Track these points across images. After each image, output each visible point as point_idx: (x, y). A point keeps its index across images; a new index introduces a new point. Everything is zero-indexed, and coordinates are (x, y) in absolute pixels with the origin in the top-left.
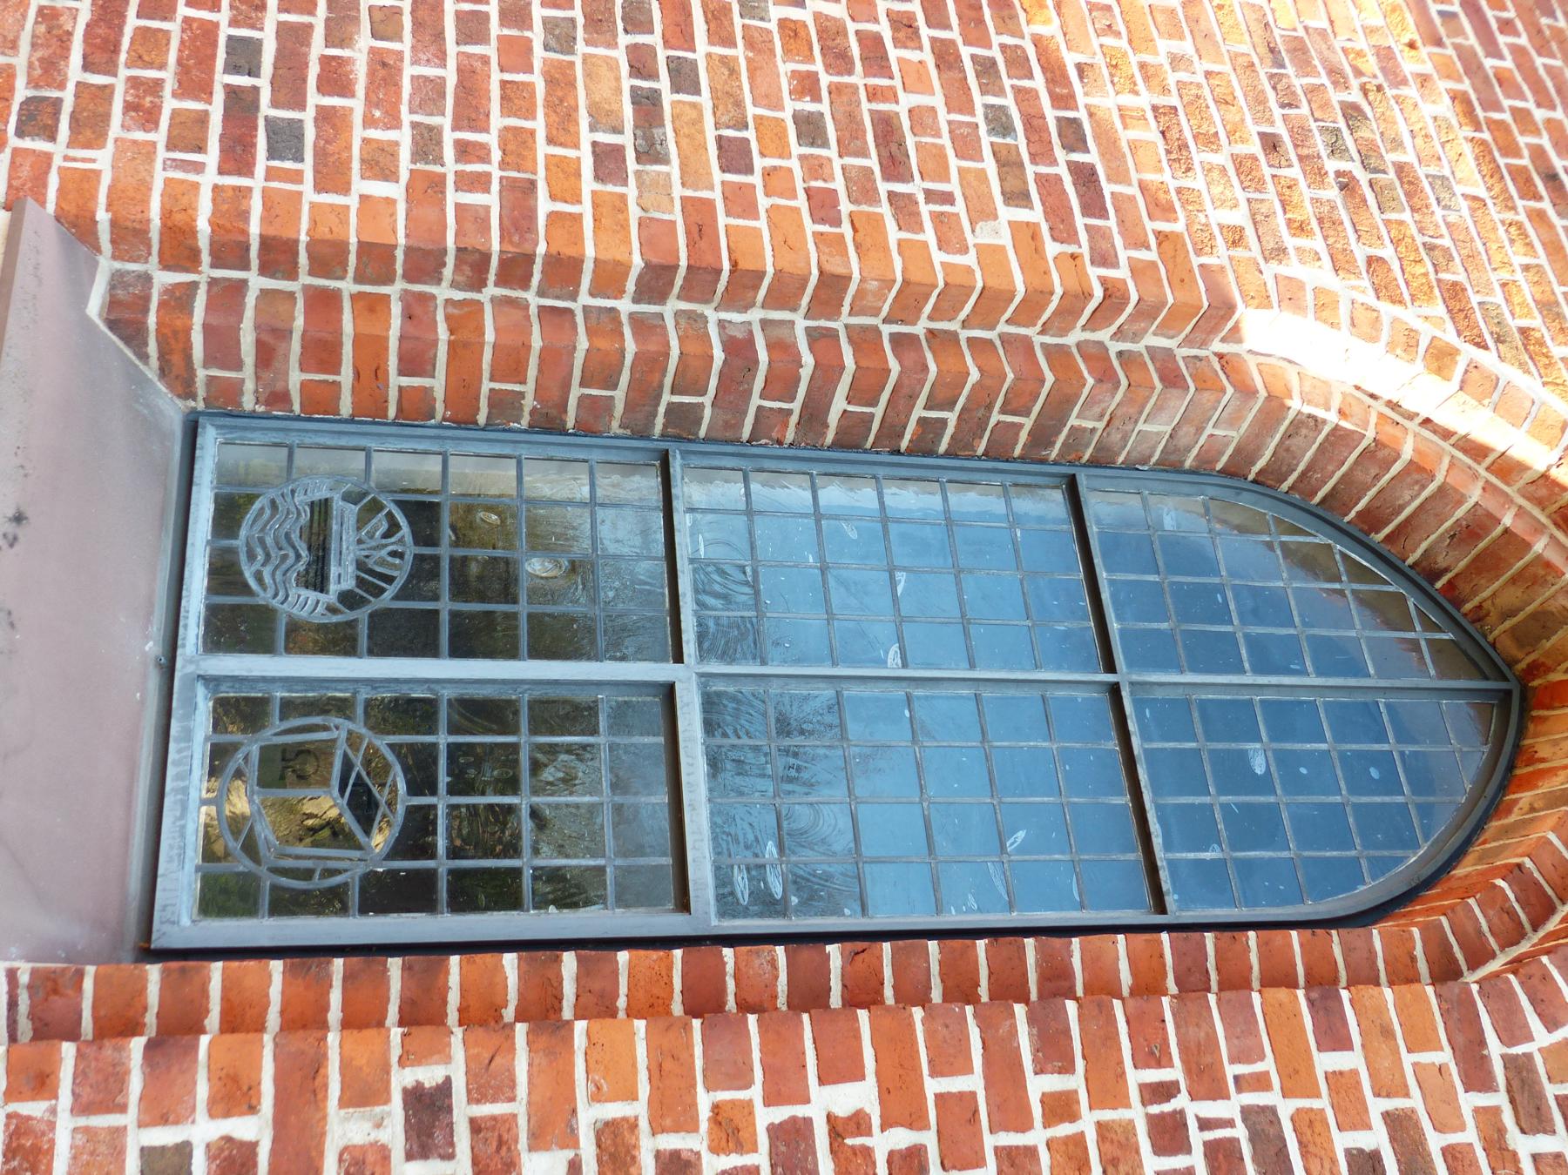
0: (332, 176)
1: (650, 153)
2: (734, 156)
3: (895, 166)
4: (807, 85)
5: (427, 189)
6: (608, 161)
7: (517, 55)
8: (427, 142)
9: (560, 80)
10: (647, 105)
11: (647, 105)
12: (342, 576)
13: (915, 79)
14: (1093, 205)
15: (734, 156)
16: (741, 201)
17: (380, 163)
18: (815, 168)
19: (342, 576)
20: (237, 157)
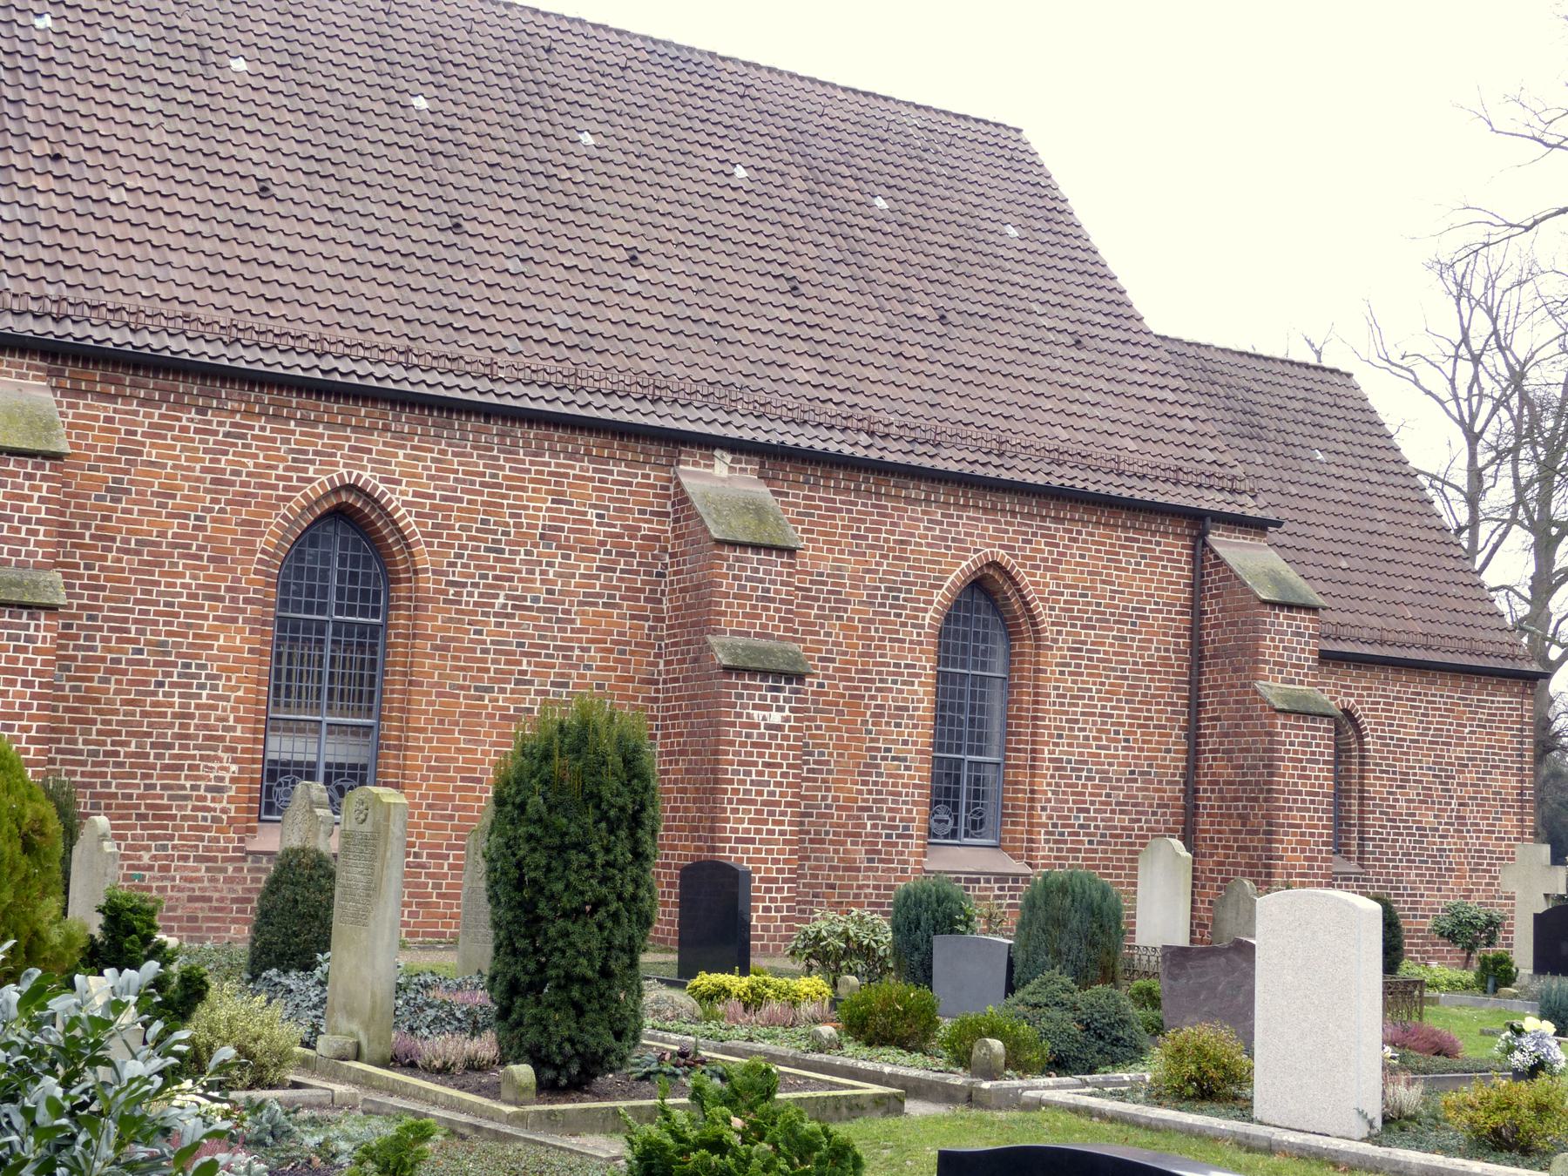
0: (913, 820)
1: (905, 760)
2: (905, 743)
3: (907, 709)
4: (888, 724)
5: (915, 803)
6: (907, 768)
7: (885, 784)
8: (905, 803)
9: (890, 776)
10: (894, 759)
11: (894, 759)
12: (946, 817)
13: (885, 699)
14: (914, 666)
15: (905, 743)
16: (915, 743)
17: (910, 811)
18: (907, 726)
19: (946, 817)
20: (911, 837)
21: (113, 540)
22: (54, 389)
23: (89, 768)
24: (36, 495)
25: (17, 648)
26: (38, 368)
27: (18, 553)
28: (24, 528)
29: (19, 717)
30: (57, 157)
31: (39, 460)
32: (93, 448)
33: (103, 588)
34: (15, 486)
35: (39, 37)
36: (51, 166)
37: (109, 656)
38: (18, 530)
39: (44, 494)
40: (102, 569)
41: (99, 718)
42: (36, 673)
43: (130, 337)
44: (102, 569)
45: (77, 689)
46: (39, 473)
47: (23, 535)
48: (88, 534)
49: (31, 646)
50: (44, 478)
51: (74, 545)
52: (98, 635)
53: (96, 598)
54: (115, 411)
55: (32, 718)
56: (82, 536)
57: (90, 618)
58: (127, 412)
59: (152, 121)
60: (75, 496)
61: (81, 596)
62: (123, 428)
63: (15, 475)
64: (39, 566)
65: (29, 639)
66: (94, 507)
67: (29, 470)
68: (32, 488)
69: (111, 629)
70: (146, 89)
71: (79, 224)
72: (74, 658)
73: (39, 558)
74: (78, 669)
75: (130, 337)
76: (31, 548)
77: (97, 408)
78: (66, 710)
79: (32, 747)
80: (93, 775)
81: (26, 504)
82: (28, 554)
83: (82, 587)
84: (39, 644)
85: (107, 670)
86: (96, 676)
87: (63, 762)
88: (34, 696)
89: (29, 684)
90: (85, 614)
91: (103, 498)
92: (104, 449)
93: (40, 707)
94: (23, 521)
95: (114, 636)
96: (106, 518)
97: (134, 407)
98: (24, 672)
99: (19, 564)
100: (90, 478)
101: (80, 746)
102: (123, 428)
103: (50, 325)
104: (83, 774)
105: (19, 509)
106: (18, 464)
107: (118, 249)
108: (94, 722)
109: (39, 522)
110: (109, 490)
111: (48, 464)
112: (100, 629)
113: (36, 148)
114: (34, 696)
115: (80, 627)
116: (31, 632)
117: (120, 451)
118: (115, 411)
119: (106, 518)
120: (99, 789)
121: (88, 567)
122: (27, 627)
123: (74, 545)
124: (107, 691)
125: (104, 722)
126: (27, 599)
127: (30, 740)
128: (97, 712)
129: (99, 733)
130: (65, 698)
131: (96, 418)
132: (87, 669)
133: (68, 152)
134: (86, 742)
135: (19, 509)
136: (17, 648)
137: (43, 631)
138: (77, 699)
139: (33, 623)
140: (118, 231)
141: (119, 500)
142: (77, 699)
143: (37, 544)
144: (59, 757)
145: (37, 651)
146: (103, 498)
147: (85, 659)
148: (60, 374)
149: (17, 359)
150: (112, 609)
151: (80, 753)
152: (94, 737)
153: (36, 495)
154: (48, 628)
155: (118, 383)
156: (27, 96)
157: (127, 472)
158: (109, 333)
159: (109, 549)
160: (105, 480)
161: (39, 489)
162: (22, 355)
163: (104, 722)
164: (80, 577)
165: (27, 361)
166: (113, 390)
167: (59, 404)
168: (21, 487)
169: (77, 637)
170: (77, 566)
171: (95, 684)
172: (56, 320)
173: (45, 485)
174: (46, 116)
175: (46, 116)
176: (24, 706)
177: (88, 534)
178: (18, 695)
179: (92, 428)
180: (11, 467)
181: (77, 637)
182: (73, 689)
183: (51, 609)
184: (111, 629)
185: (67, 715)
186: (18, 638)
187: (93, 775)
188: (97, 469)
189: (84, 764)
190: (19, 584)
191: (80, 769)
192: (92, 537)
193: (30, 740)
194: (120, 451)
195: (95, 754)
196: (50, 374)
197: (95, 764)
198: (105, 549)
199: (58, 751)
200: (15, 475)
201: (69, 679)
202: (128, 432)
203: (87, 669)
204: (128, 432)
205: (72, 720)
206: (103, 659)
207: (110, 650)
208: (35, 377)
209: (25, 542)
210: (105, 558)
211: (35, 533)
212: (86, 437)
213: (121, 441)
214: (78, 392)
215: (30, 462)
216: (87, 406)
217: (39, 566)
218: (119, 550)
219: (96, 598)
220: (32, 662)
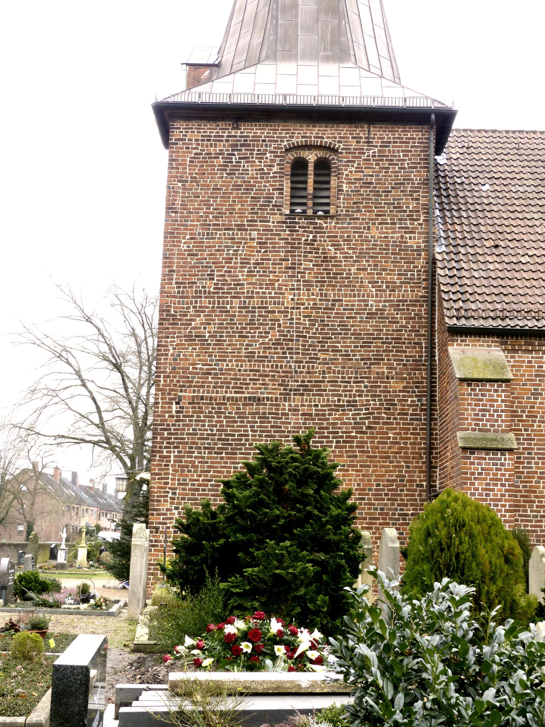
21: (536, 417)
22: (504, 350)
23: (534, 523)
24: (500, 399)
25: (497, 469)
26: (496, 342)
27: (494, 426)
28: (496, 414)
29: (500, 500)
30: (497, 246)
31: (500, 383)
32: (523, 375)
33: (534, 440)
34: (490, 396)
35: (484, 194)
36: (494, 251)
37: (539, 471)
38: (493, 416)
39: (503, 398)
40: (532, 431)
41: (536, 500)
42: (506, 480)
43: (536, 323)
44: (532, 431)
45: (526, 487)
46: (500, 389)
47: (495, 417)
48: (524, 415)
49: (503, 468)
50: (503, 391)
51: (518, 421)
52: (533, 461)
53: (531, 444)
54: (532, 357)
55: (506, 500)
56: (522, 416)
57: (529, 453)
58: (537, 358)
59: (537, 223)
60: (518, 398)
61: (524, 444)
62: (536, 365)
63: (489, 391)
64: (503, 431)
65: (502, 465)
66: (526, 403)
67: (496, 388)
68: (498, 396)
69: (539, 458)
70: (534, 209)
71: (509, 275)
72: (523, 473)
73: (503, 428)
74: (525, 477)
75: (536, 323)
76: (499, 423)
77: (524, 357)
78: (522, 496)
79: (507, 514)
80: (536, 526)
81: (495, 404)
82: (498, 426)
83: (524, 439)
84: (507, 467)
85: (538, 478)
86: (534, 480)
87: (522, 521)
88: (506, 491)
89: (503, 485)
90: (526, 452)
91: (530, 398)
92: (528, 375)
93: (509, 496)
94: (496, 411)
95: (540, 461)
96: (532, 407)
97: (541, 355)
98: (501, 480)
99: (495, 431)
100: (524, 389)
101: (529, 513)
102: (536, 365)
103: (500, 322)
104: (531, 526)
105: (493, 406)
106: (491, 385)
107: (528, 284)
108: (534, 502)
109: (502, 411)
110: (532, 394)
111: (504, 385)
112: (534, 458)
113: (487, 244)
114: (506, 491)
115: (524, 458)
116: (503, 461)
117: (536, 376)
118: (532, 357)
119: (532, 407)
120: (539, 533)
121: (526, 430)
122: (500, 459)
123: (518, 421)
124: (539, 487)
125: (539, 502)
126: (500, 446)
127: (506, 511)
128: (536, 497)
129: (537, 507)
130: (520, 491)
131: (523, 362)
132: (529, 477)
133: (501, 243)
134: (531, 511)
135: (493, 406)
136: (497, 469)
137: (508, 460)
138: (525, 491)
139: (503, 457)
140: (526, 275)
141: (537, 399)
142: (525, 491)
143: (502, 421)
144: (520, 518)
145: (506, 470)
146: (530, 398)
147: (528, 473)
148: (506, 343)
149: (486, 339)
150: (538, 449)
151: (529, 516)
152: (535, 508)
153: (500, 399)
154: (510, 459)
155: (532, 345)
156: (481, 221)
157: (540, 385)
158: (526, 322)
159: (535, 421)
160: (530, 390)
161: (501, 396)
162: (489, 337)
163: (539, 502)
164: (523, 435)
165: (491, 339)
166: (530, 348)
167: (507, 357)
168: (493, 396)
169: (523, 463)
170: (521, 430)
171: (533, 484)
172: (502, 319)
173: (503, 394)
174: (490, 229)
175: (490, 229)
176: (502, 495)
177: (524, 415)
178: (499, 490)
179: (522, 366)
180: (488, 387)
181: (523, 463)
182: (524, 487)
183: (511, 450)
184: (539, 458)
185: (522, 499)
186: (497, 465)
187: (536, 526)
188: (526, 385)
189: (531, 521)
190: (495, 440)
191: (530, 524)
192: (527, 416)
193: (506, 511)
194: (536, 376)
195: (535, 516)
196: (502, 344)
197: (536, 521)
198: (533, 421)
199: (519, 516)
200: (489, 391)
201: (521, 482)
202: (539, 367)
203: (529, 477)
204: (539, 367)
205: (524, 501)
206: (536, 473)
207: (539, 468)
208: (495, 346)
209: (497, 421)
210: (533, 426)
211: (500, 416)
212: (520, 371)
213: (536, 371)
214: (515, 351)
215: (496, 384)
216: (519, 357)
217: (503, 431)
218: (539, 421)
219: (531, 444)
220: (504, 475)
